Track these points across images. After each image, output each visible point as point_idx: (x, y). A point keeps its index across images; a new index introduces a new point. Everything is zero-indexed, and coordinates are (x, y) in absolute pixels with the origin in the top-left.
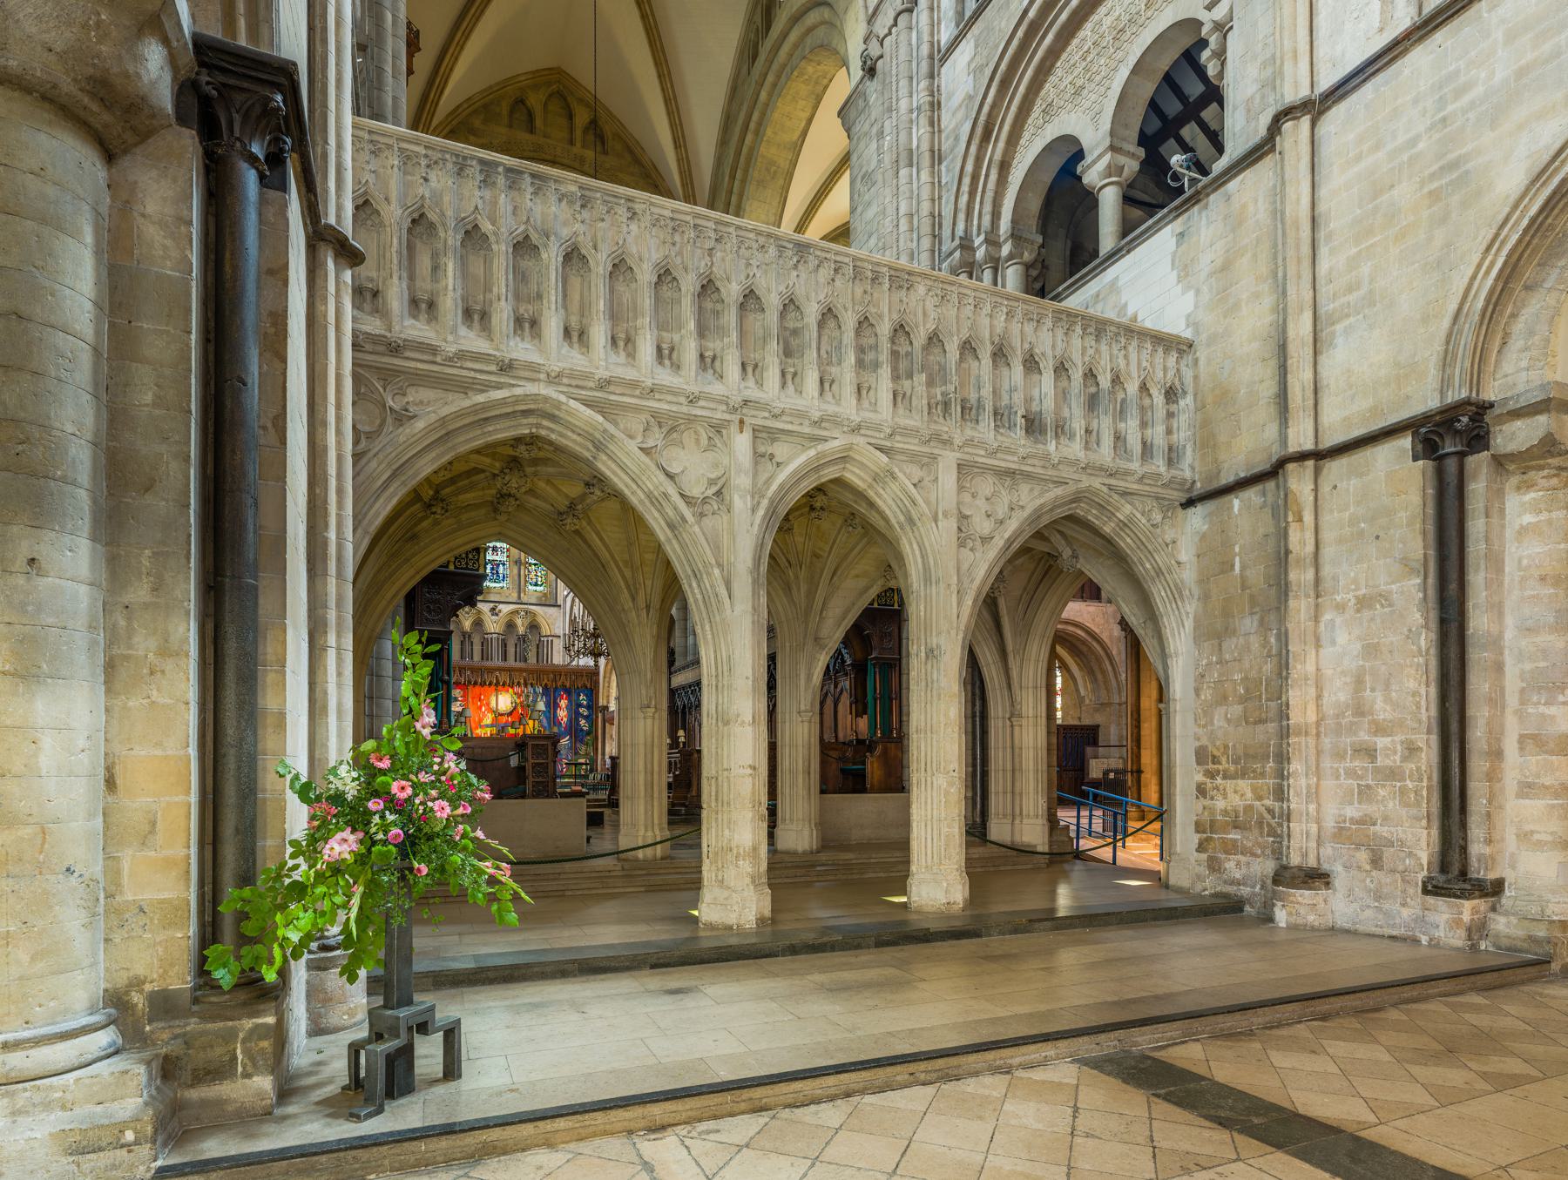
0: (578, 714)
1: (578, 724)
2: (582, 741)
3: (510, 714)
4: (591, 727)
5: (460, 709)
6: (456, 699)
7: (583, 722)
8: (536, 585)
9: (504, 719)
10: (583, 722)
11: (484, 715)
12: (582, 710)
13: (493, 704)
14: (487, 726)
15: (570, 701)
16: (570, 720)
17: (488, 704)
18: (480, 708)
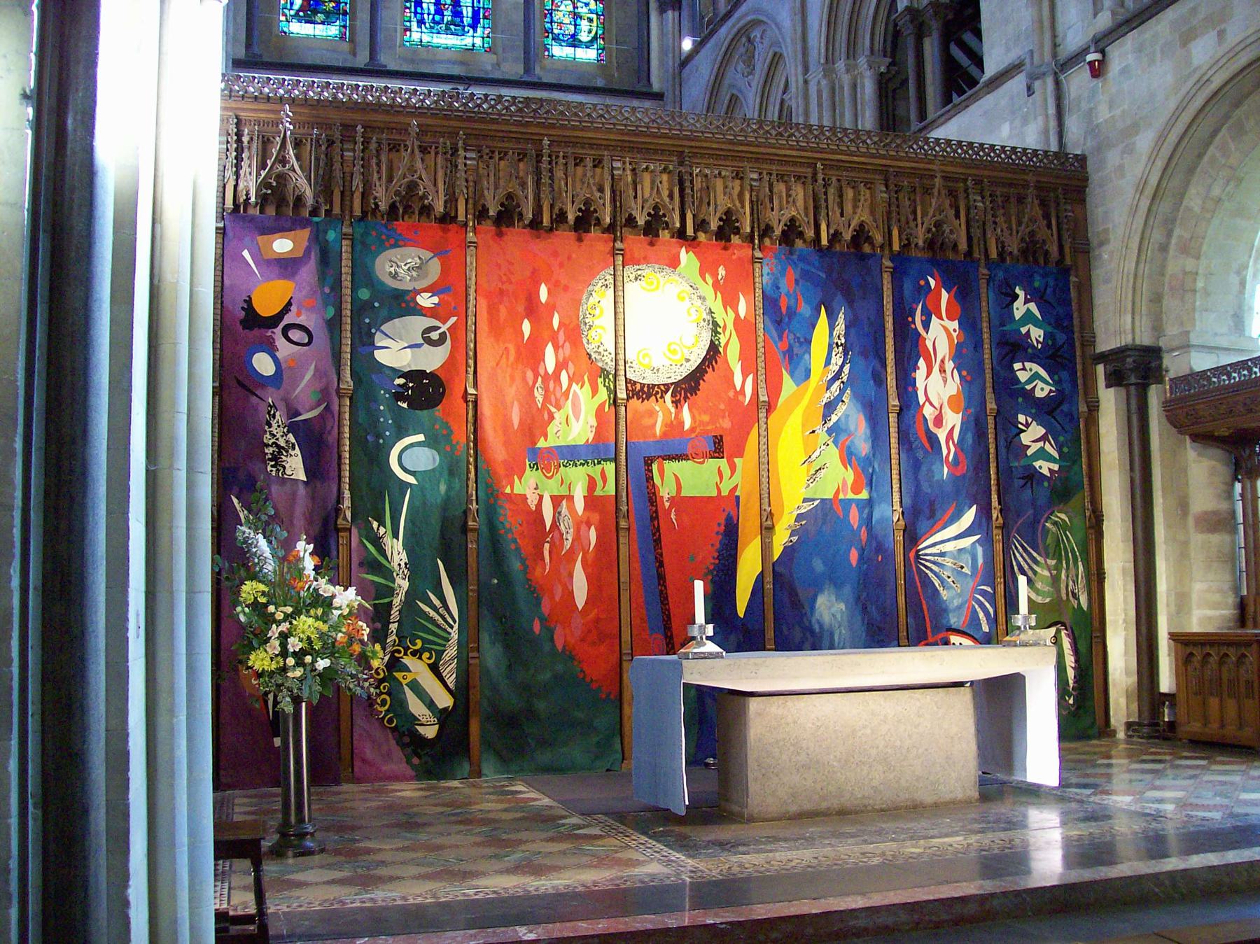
0: (1009, 390)
1: (1012, 444)
2: (1033, 536)
3: (689, 386)
4: (1069, 457)
5: (432, 360)
6: (402, 304)
7: (1032, 434)
8: (574, 42)
9: (661, 412)
10: (1032, 434)
11: (555, 399)
12: (1025, 371)
13: (600, 336)
14: (572, 455)
15: (969, 324)
16: (975, 425)
17: (574, 333)
18: (532, 354)
